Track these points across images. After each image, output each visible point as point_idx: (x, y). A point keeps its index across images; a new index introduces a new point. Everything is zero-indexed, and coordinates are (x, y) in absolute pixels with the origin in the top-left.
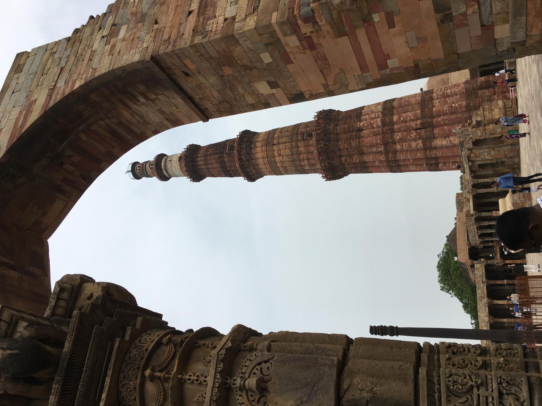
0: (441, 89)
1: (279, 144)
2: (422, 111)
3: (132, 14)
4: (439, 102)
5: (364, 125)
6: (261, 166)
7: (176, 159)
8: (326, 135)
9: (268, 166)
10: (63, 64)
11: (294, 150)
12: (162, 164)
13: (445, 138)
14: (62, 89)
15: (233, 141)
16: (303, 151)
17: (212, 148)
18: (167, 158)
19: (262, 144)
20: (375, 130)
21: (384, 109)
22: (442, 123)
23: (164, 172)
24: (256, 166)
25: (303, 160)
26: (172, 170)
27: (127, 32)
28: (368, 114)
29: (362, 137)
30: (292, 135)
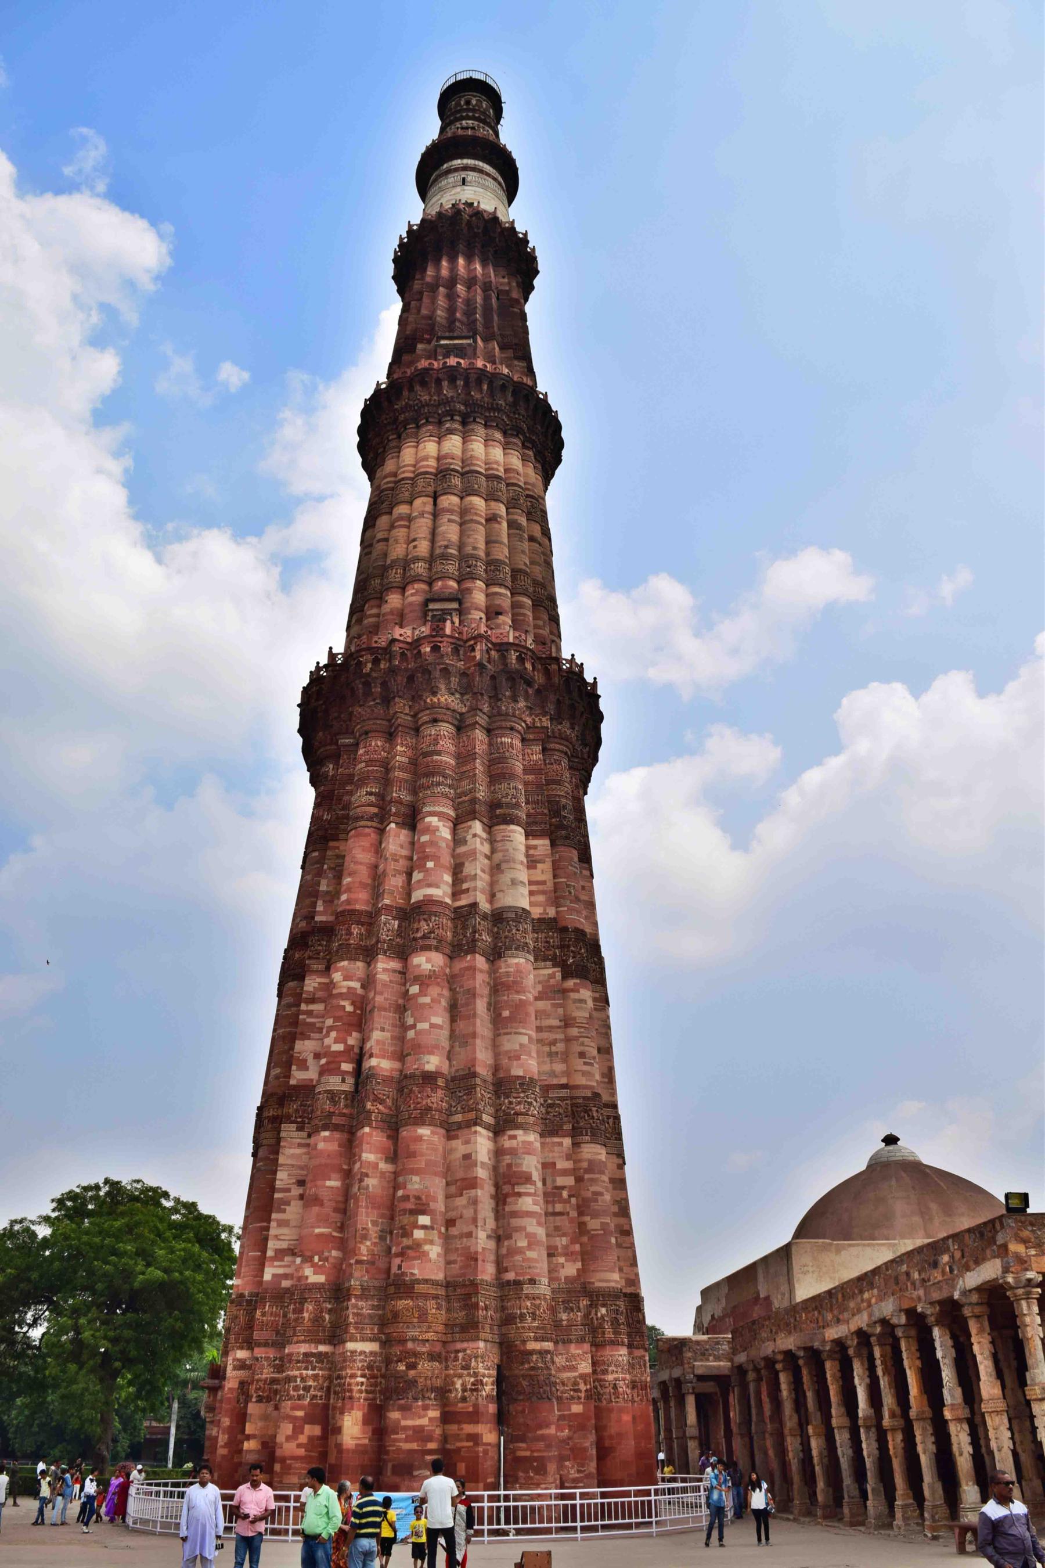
0: (565, 1173)
1: (435, 515)
2: (429, 1078)
4: (467, 1157)
5: (430, 830)
8: (411, 679)
11: (395, 576)
12: (459, 161)
13: (301, 1183)
16: (386, 608)
17: (487, 299)
18: (481, 171)
19: (446, 456)
20: (395, 882)
21: (498, 917)
22: (357, 1165)
28: (493, 851)
29: (382, 831)
30: (465, 559)
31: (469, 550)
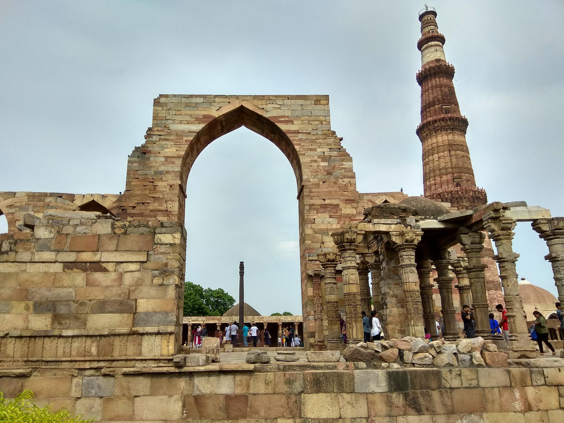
1: (451, 156)
3: (334, 166)
6: (430, 141)
7: (438, 55)
9: (430, 147)
10: (314, 132)
11: (443, 171)
14: (297, 138)
15: (457, 110)
16: (443, 179)
17: (449, 90)
19: (450, 140)
23: (425, 46)
24: (430, 135)
25: (435, 180)
26: (427, 53)
27: (323, 167)
30: (458, 167)
31: (460, 165)
